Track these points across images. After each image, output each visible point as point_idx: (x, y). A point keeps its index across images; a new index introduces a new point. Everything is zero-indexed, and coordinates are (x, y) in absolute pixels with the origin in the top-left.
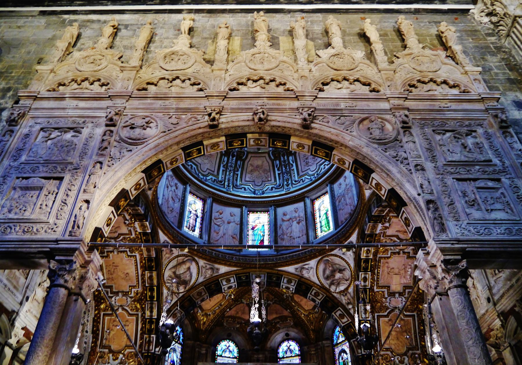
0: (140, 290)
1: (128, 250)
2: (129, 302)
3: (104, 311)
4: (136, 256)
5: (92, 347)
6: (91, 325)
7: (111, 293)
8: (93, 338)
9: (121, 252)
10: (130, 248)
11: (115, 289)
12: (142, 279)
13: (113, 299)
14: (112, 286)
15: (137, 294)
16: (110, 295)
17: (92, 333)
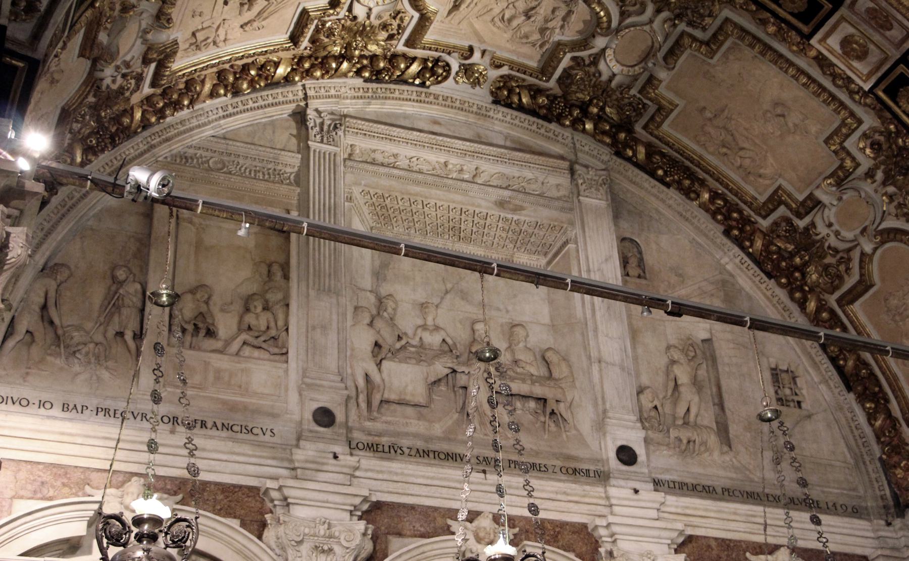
0: (869, 121)
1: (682, 26)
2: (876, 197)
3: (834, 289)
4: (727, 20)
5: (879, 435)
6: (826, 364)
7: (800, 216)
8: (862, 398)
9: (672, 53)
10: (679, 16)
11: (800, 191)
12: (834, 77)
13: (822, 230)
14: (779, 187)
15: (876, 146)
16: (801, 224)
17: (849, 389)
